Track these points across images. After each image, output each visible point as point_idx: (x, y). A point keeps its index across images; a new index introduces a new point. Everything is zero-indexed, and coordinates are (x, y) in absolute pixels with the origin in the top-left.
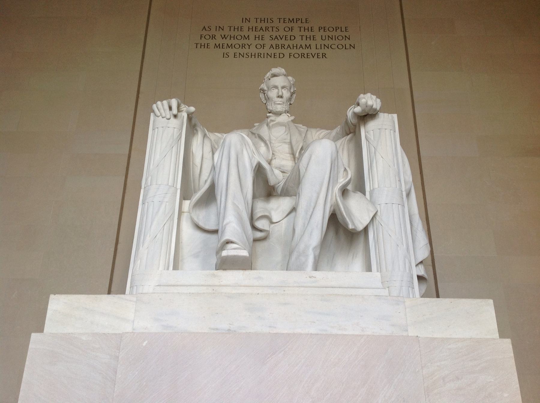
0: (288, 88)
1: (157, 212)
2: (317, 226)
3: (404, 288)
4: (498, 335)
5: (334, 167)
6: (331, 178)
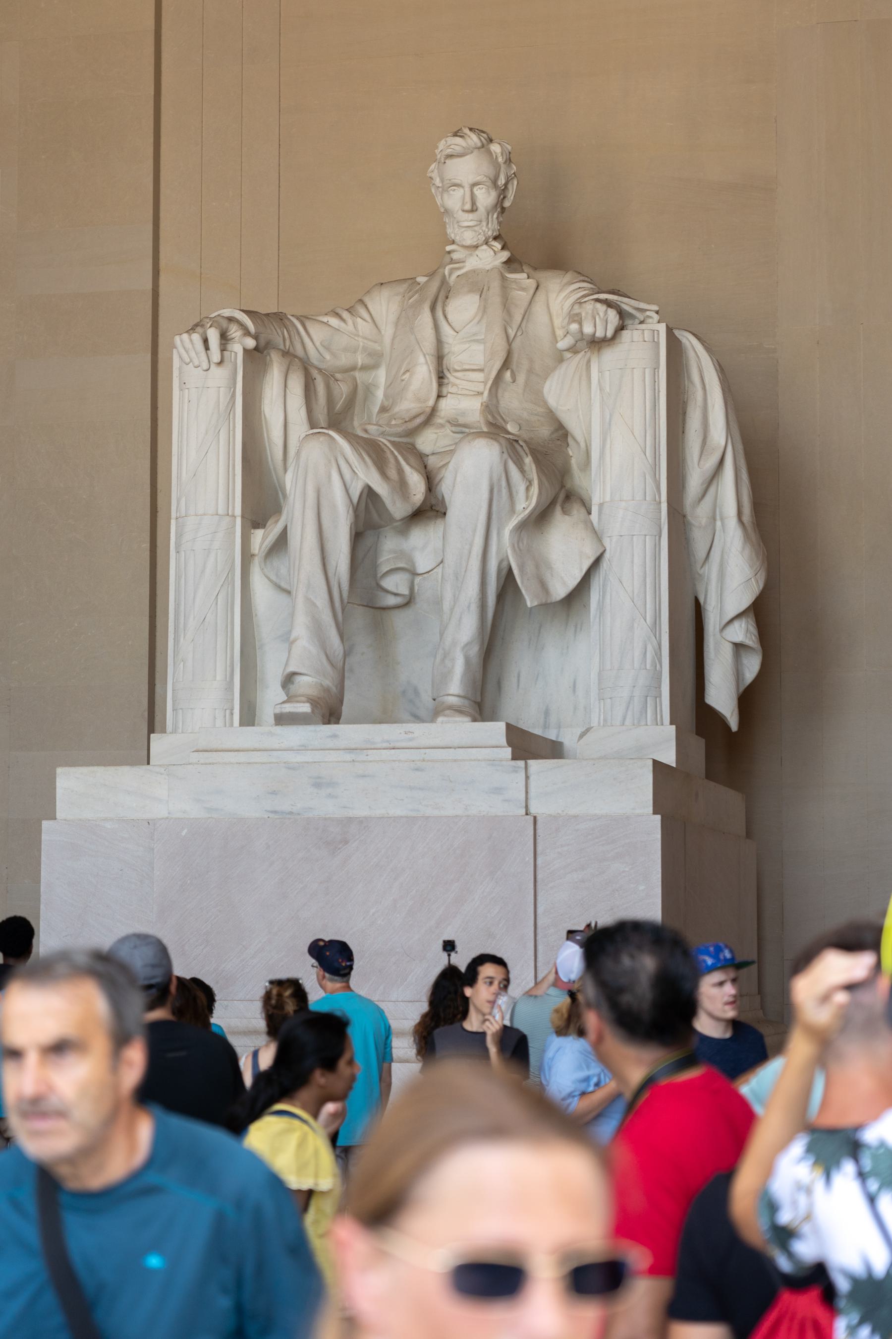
0: (489, 183)
1: (203, 572)
2: (469, 607)
3: (636, 699)
4: (651, 808)
5: (500, 491)
6: (494, 516)
